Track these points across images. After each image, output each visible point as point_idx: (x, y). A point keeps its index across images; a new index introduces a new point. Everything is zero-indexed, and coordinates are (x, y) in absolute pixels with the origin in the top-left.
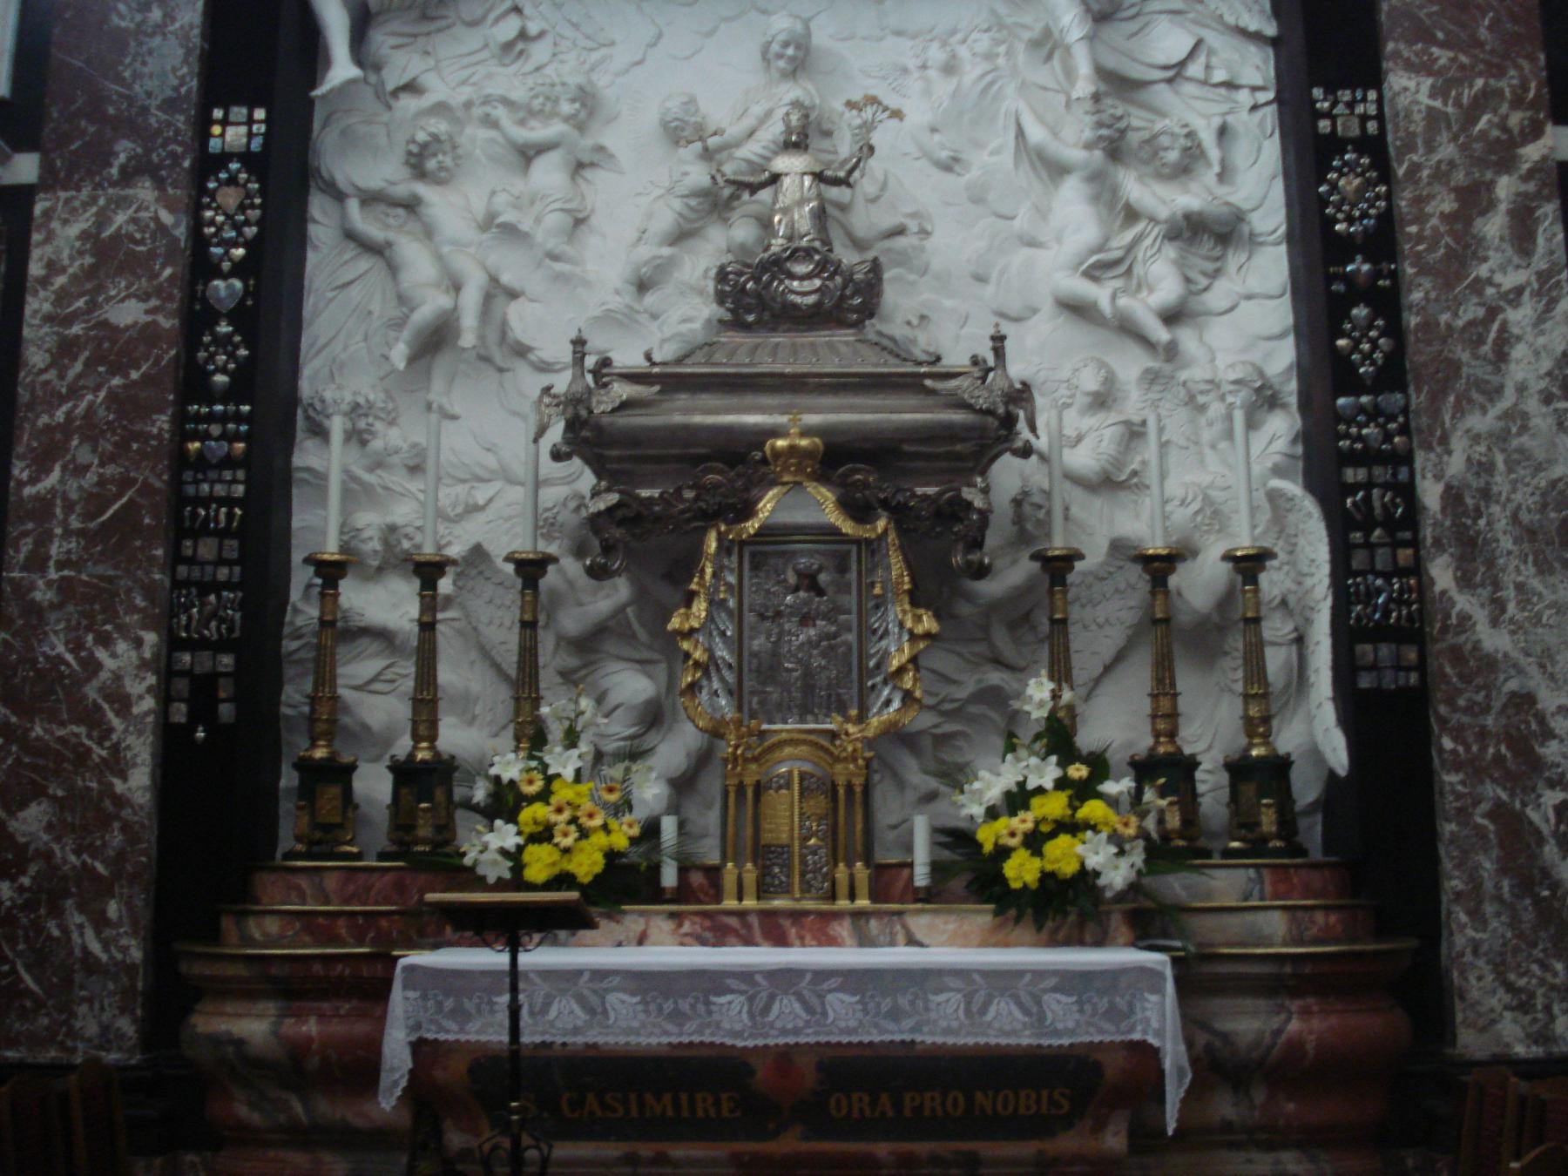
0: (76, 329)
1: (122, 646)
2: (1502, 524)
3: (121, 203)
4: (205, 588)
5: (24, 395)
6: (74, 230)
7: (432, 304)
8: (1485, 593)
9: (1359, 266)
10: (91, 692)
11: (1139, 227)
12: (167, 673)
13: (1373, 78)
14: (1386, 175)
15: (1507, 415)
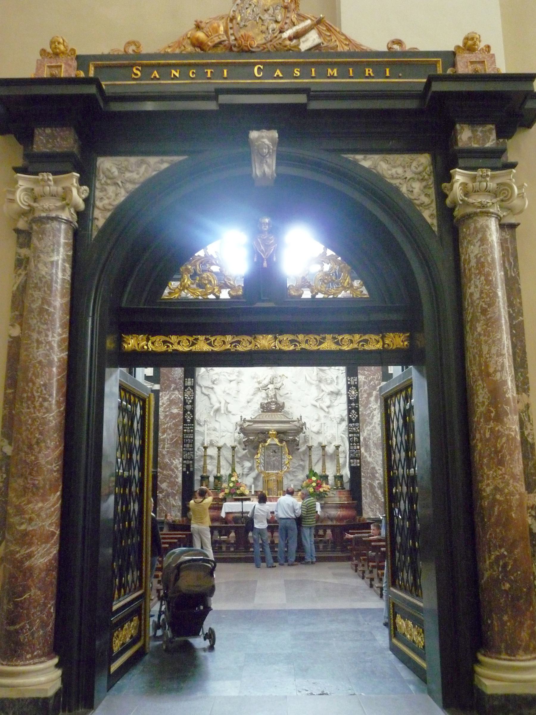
0: (167, 413)
1: (177, 460)
2: (371, 443)
3: (173, 394)
5: (160, 423)
6: (166, 398)
7: (217, 405)
8: (369, 453)
9: (353, 404)
10: (172, 467)
11: (324, 393)
12: (183, 464)
13: (357, 376)
14: (358, 391)
15: (373, 427)
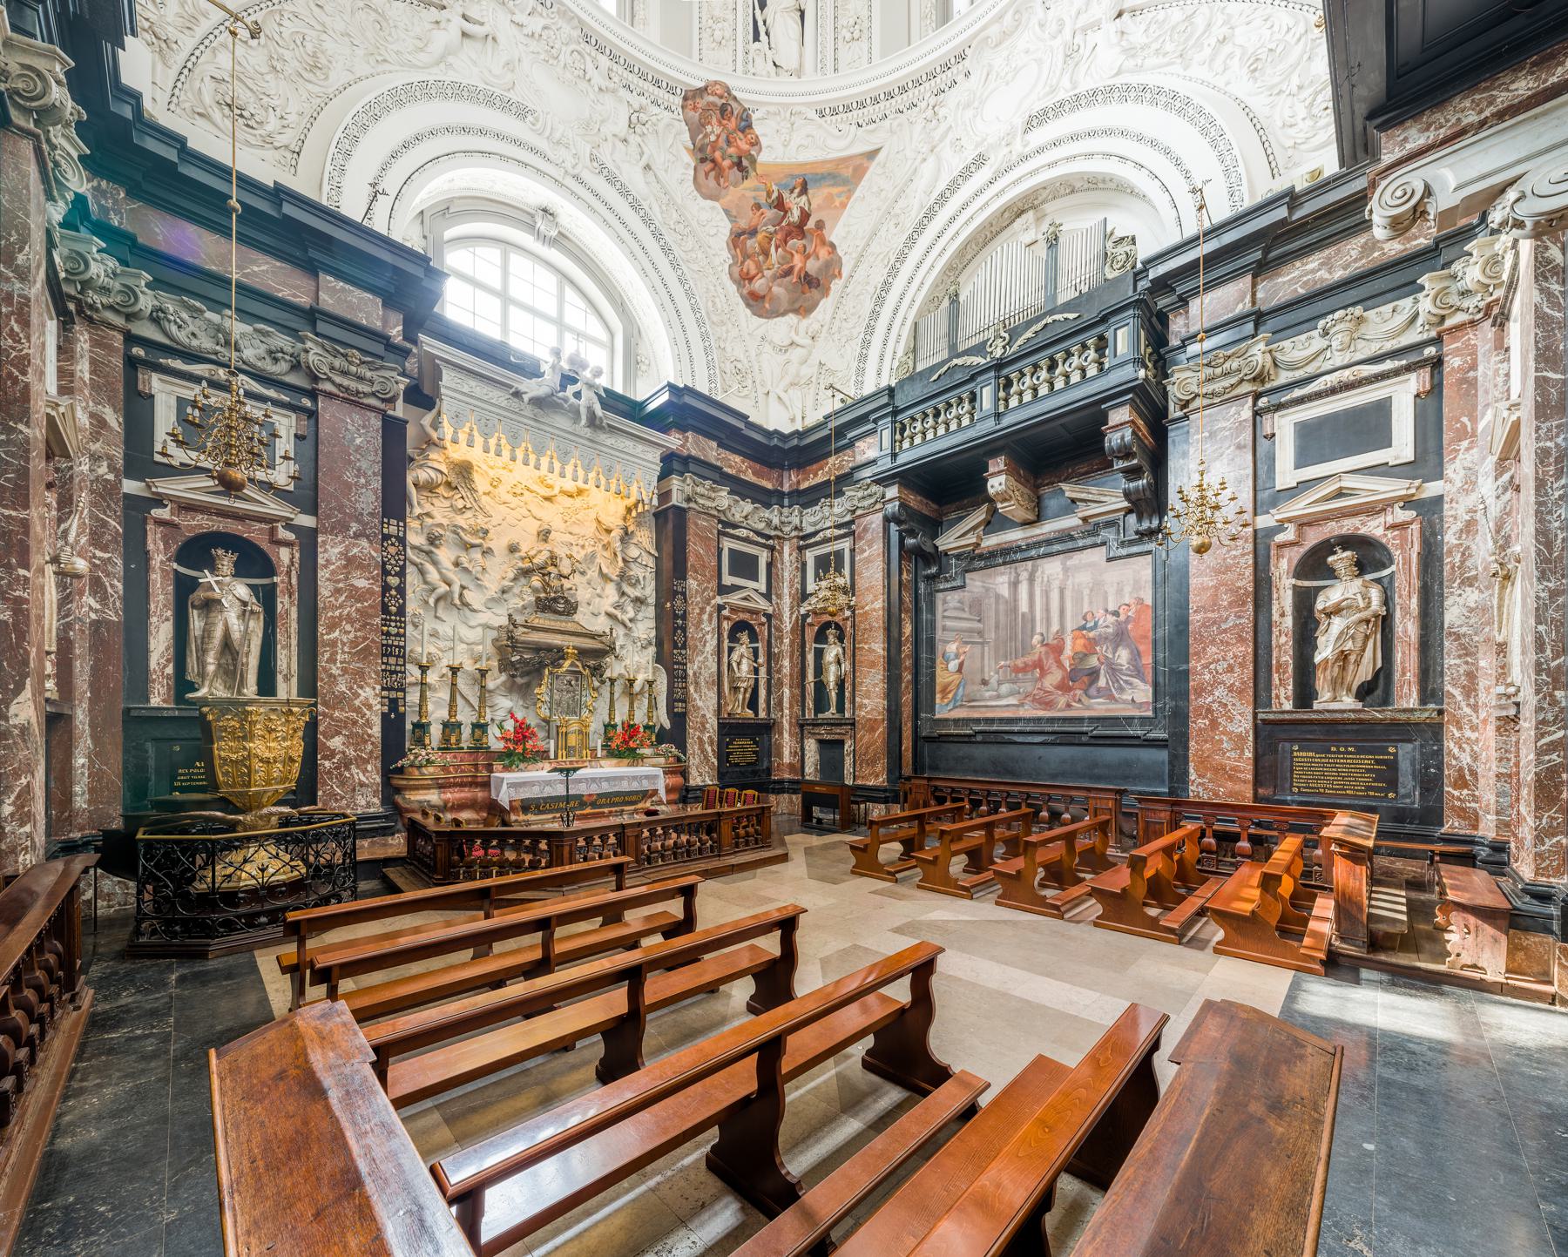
4: (392, 672)
5: (321, 605)
6: (337, 550)
7: (443, 588)
